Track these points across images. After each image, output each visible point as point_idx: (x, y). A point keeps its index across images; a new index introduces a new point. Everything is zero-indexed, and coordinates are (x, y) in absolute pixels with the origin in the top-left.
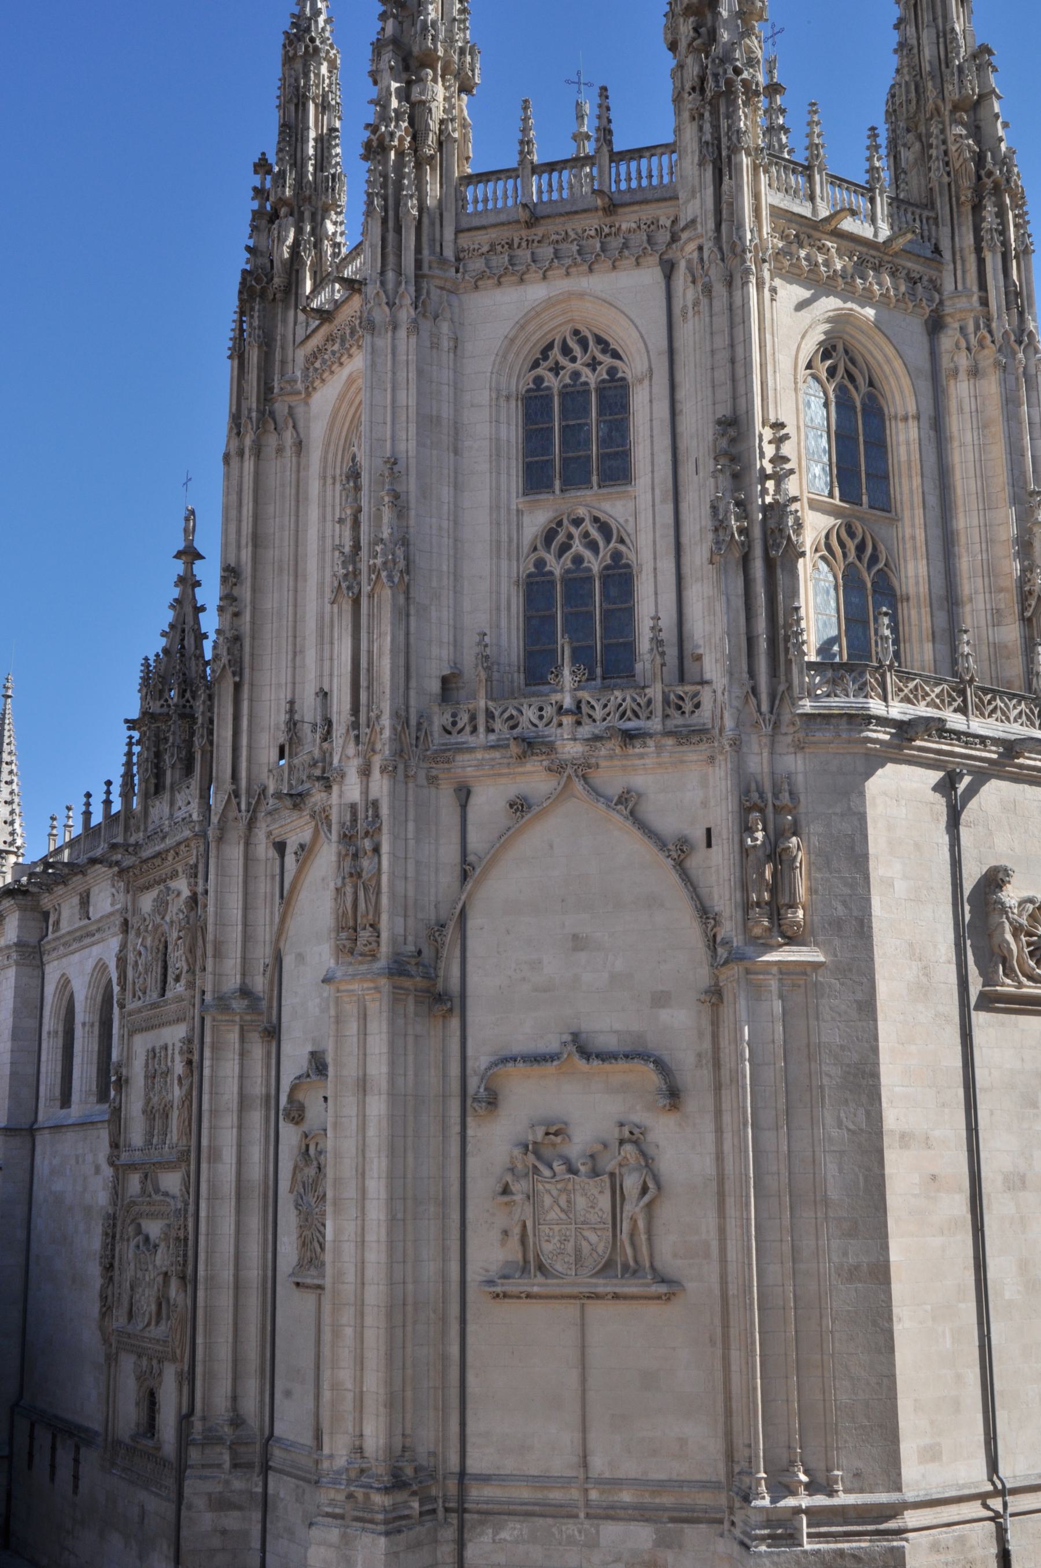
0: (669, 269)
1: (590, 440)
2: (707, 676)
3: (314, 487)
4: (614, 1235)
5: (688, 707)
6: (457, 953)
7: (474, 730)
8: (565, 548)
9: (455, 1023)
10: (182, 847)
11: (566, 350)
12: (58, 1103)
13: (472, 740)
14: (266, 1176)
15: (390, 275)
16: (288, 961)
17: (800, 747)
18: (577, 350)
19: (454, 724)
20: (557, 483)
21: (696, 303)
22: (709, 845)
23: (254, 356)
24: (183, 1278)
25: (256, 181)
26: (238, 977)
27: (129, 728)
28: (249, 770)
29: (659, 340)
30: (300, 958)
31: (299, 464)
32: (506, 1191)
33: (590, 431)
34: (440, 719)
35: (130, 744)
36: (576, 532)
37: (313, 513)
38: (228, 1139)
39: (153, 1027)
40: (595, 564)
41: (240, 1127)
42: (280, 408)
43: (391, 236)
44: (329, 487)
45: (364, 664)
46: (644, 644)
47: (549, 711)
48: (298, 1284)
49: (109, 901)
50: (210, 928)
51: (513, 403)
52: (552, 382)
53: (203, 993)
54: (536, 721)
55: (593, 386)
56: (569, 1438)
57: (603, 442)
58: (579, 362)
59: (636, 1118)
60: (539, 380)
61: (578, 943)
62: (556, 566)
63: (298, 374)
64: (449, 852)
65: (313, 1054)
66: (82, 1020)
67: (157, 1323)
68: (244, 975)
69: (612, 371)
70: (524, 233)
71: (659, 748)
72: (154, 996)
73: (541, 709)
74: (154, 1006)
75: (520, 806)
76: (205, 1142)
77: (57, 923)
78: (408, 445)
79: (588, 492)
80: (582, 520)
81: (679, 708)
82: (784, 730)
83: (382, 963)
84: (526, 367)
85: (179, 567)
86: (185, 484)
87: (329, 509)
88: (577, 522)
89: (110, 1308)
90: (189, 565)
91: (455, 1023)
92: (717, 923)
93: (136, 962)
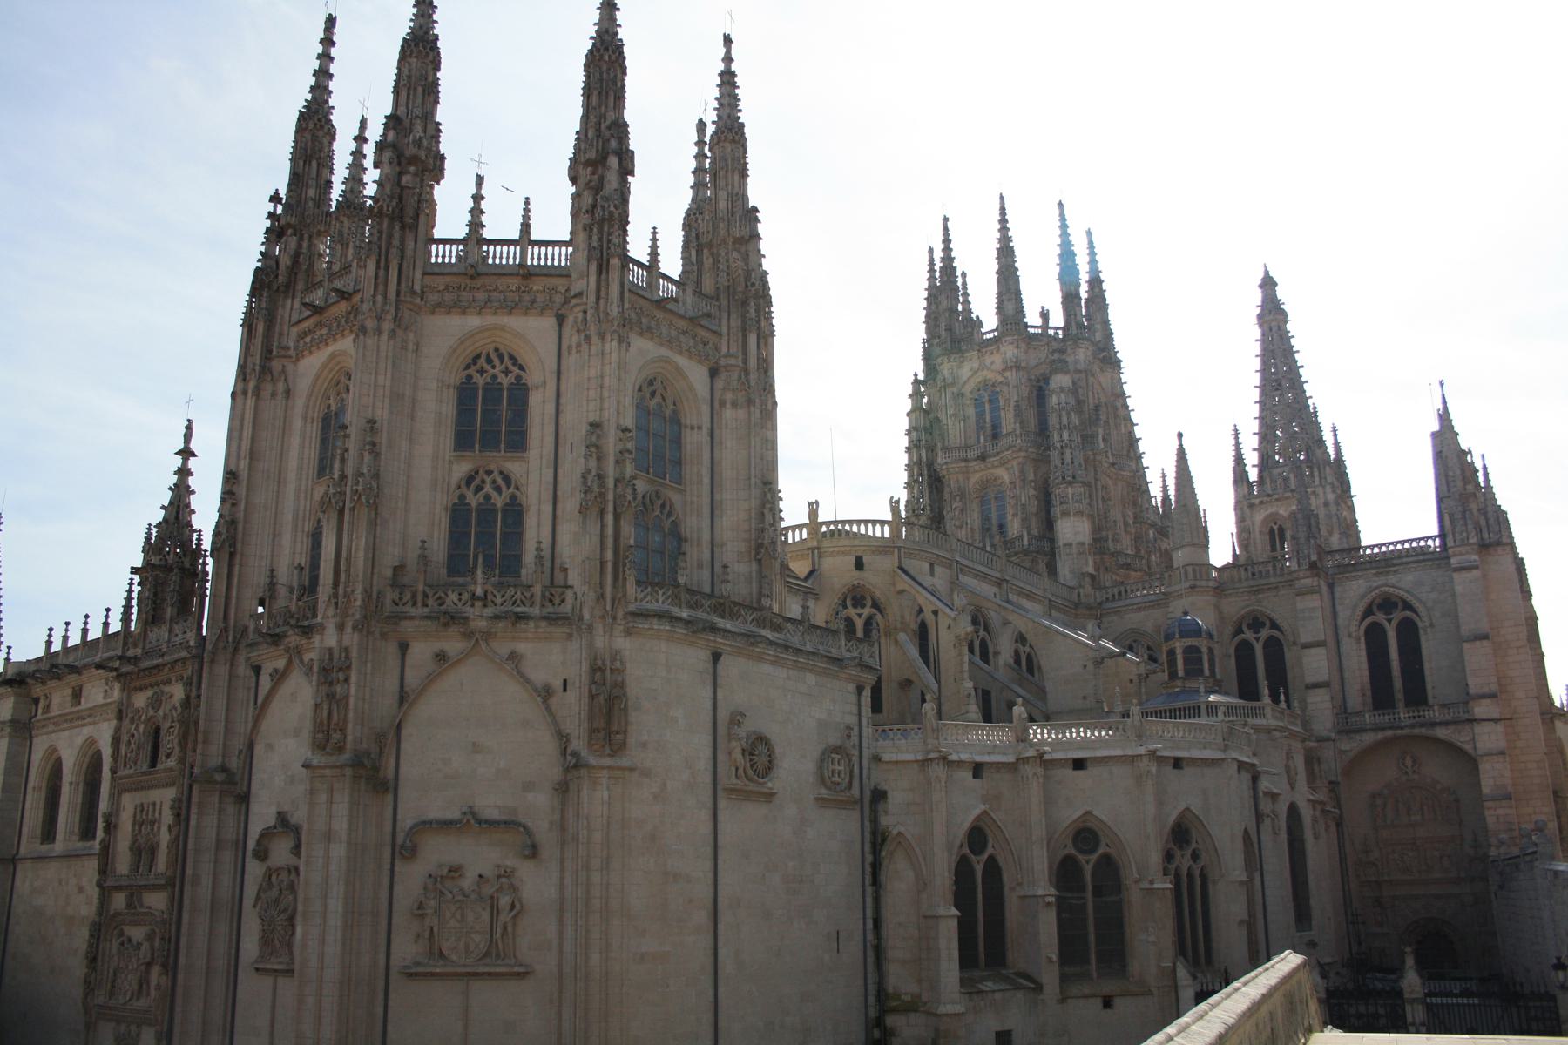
0: (561, 320)
1: (499, 422)
2: (570, 583)
3: (297, 423)
4: (491, 936)
5: (557, 601)
6: (394, 750)
7: (414, 604)
8: (479, 489)
9: (390, 797)
10: (179, 664)
11: (489, 361)
12: (39, 841)
13: (413, 611)
14: (233, 897)
15: (379, 298)
16: (259, 749)
17: (628, 633)
18: (497, 362)
19: (401, 599)
20: (477, 446)
21: (579, 345)
22: (565, 690)
23: (261, 328)
24: (164, 966)
25: (270, 207)
26: (220, 758)
27: (132, 573)
28: (236, 614)
30: (270, 747)
31: (286, 406)
32: (421, 906)
33: (501, 415)
34: (390, 595)
35: (131, 584)
36: (488, 479)
37: (295, 441)
39: (143, 788)
40: (499, 501)
41: (216, 862)
42: (276, 365)
43: (382, 272)
44: (309, 425)
45: (344, 554)
46: (529, 557)
47: (465, 596)
48: (257, 970)
49: (102, 695)
51: (451, 390)
52: (480, 380)
53: (192, 767)
54: (456, 601)
55: (505, 386)
57: (509, 424)
58: (497, 369)
59: (508, 863)
60: (469, 377)
62: (473, 500)
63: (291, 344)
64: (392, 685)
65: (279, 813)
66: (69, 780)
67: (138, 999)
68: (223, 756)
69: (518, 378)
70: (468, 281)
71: (537, 627)
72: (145, 767)
73: (460, 594)
74: (144, 773)
75: (441, 657)
76: (189, 871)
77: (47, 708)
78: (382, 413)
79: (497, 454)
80: (492, 472)
82: (619, 621)
83: (346, 756)
84: (463, 367)
85: (178, 461)
86: (188, 402)
87: (307, 440)
88: (489, 473)
90: (185, 461)
91: (390, 797)
92: (568, 740)
93: (129, 742)
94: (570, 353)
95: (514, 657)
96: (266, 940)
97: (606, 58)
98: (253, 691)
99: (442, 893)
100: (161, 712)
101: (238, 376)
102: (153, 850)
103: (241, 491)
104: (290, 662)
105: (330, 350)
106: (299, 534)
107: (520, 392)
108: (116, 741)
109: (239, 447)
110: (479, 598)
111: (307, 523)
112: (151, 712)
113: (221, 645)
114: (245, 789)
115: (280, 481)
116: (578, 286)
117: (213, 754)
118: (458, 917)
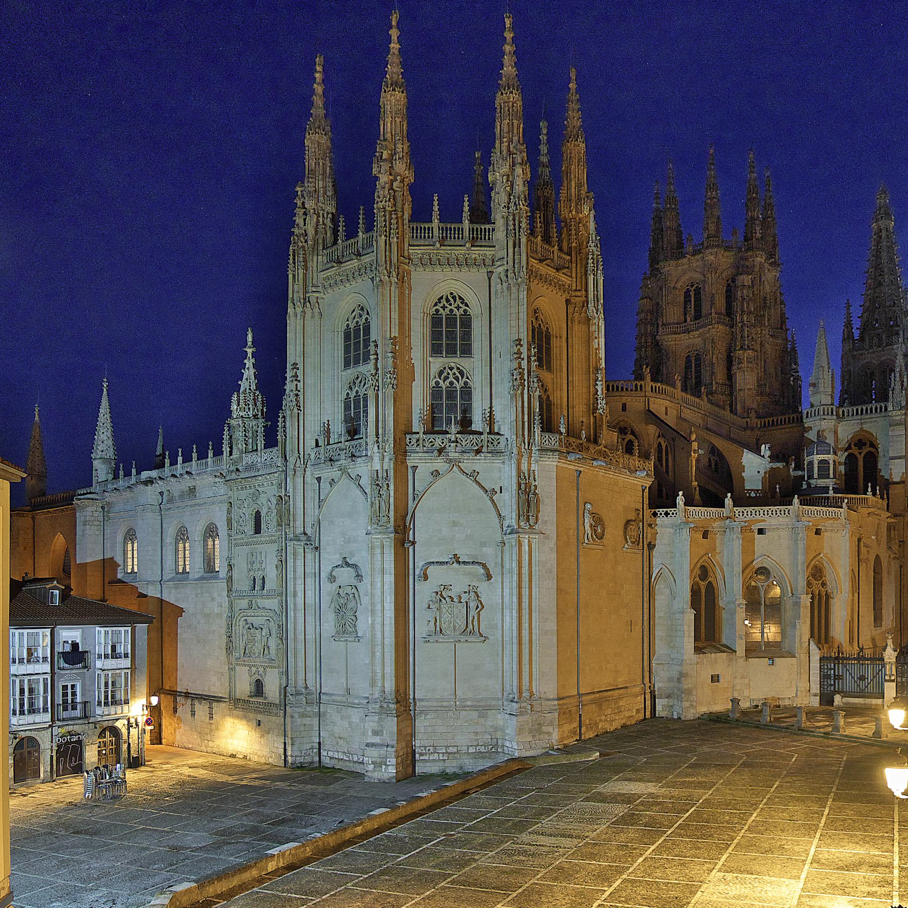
5: (495, 444)
8: (446, 378)
22: (501, 492)
40: (458, 386)
61: (455, 524)
73: (443, 440)
81: (492, 443)
88: (451, 369)
107: (467, 322)
111: (340, 396)
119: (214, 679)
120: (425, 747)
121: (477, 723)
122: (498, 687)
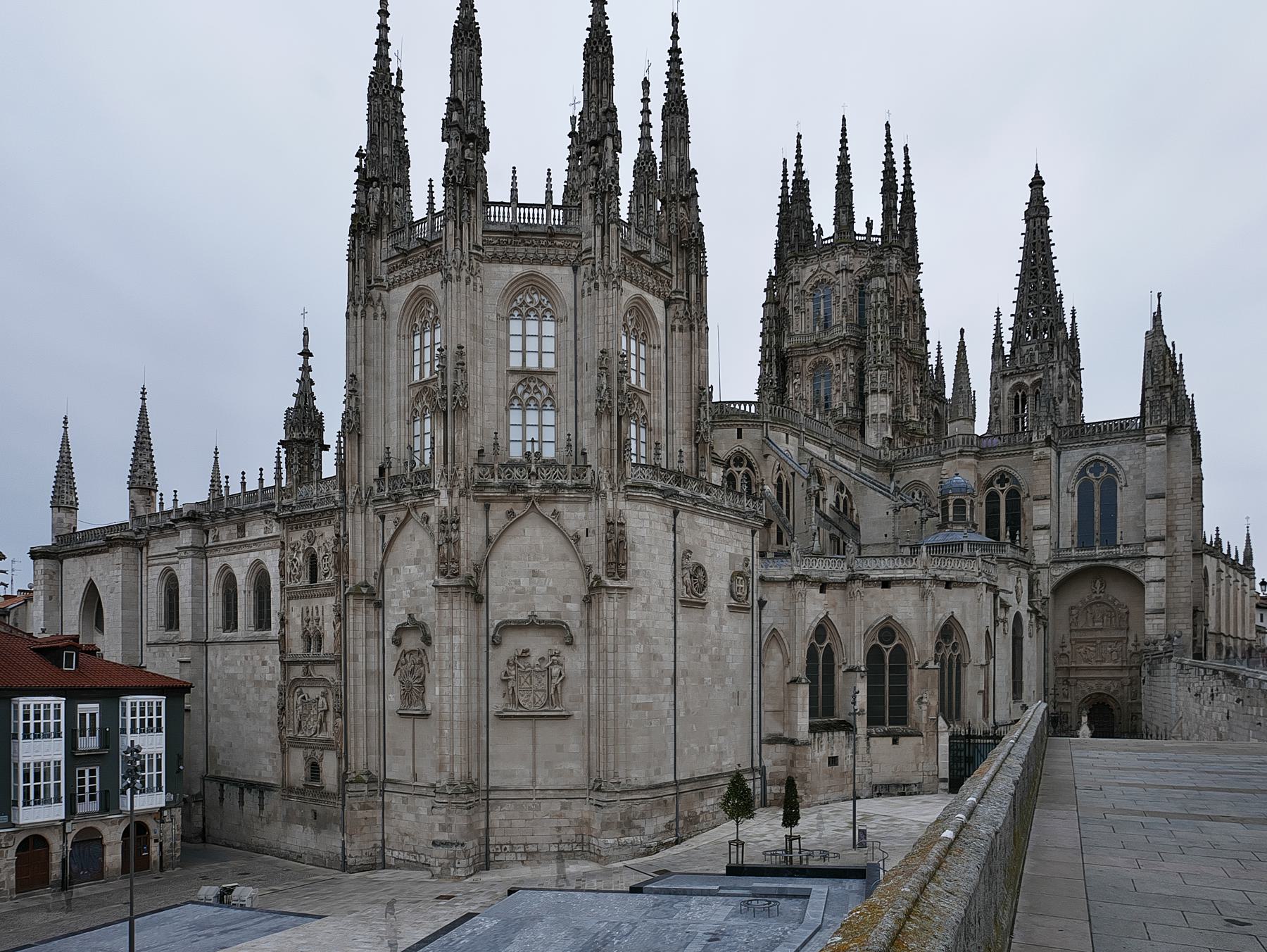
0: (575, 269)
10: (328, 512)
12: (222, 630)
16: (388, 572)
17: (628, 499)
21: (589, 290)
29: (570, 302)
30: (396, 571)
38: (361, 651)
44: (402, 341)
48: (400, 714)
50: (350, 554)
56: (528, 771)
59: (556, 647)
61: (535, 574)
72: (305, 581)
75: (510, 514)
87: (402, 351)
89: (285, 727)
94: (583, 296)
95: (555, 513)
96: (406, 695)
97: (601, 50)
98: (381, 532)
99: (519, 667)
100: (315, 547)
101: (349, 300)
102: (320, 638)
103: (361, 390)
104: (409, 512)
105: (415, 284)
106: (403, 421)
108: (282, 564)
109: (356, 356)
110: (533, 474)
112: (307, 545)
113: (357, 500)
114: (381, 598)
115: (386, 382)
116: (587, 244)
117: (358, 575)
118: (528, 680)
119: (266, 761)
120: (501, 845)
121: (560, 816)
122: (583, 772)
